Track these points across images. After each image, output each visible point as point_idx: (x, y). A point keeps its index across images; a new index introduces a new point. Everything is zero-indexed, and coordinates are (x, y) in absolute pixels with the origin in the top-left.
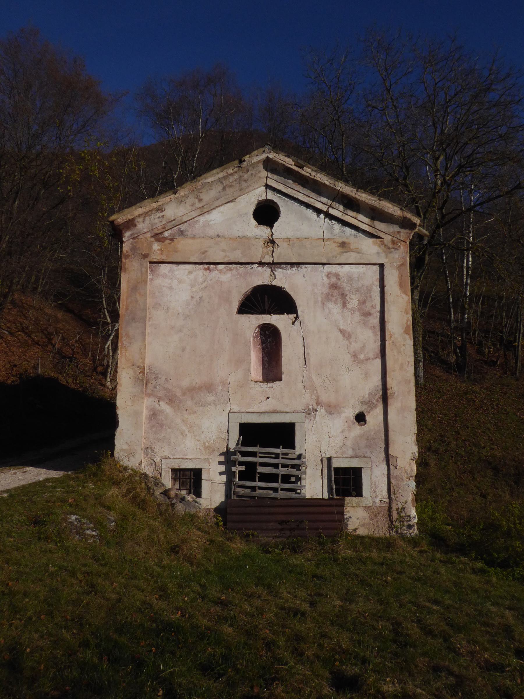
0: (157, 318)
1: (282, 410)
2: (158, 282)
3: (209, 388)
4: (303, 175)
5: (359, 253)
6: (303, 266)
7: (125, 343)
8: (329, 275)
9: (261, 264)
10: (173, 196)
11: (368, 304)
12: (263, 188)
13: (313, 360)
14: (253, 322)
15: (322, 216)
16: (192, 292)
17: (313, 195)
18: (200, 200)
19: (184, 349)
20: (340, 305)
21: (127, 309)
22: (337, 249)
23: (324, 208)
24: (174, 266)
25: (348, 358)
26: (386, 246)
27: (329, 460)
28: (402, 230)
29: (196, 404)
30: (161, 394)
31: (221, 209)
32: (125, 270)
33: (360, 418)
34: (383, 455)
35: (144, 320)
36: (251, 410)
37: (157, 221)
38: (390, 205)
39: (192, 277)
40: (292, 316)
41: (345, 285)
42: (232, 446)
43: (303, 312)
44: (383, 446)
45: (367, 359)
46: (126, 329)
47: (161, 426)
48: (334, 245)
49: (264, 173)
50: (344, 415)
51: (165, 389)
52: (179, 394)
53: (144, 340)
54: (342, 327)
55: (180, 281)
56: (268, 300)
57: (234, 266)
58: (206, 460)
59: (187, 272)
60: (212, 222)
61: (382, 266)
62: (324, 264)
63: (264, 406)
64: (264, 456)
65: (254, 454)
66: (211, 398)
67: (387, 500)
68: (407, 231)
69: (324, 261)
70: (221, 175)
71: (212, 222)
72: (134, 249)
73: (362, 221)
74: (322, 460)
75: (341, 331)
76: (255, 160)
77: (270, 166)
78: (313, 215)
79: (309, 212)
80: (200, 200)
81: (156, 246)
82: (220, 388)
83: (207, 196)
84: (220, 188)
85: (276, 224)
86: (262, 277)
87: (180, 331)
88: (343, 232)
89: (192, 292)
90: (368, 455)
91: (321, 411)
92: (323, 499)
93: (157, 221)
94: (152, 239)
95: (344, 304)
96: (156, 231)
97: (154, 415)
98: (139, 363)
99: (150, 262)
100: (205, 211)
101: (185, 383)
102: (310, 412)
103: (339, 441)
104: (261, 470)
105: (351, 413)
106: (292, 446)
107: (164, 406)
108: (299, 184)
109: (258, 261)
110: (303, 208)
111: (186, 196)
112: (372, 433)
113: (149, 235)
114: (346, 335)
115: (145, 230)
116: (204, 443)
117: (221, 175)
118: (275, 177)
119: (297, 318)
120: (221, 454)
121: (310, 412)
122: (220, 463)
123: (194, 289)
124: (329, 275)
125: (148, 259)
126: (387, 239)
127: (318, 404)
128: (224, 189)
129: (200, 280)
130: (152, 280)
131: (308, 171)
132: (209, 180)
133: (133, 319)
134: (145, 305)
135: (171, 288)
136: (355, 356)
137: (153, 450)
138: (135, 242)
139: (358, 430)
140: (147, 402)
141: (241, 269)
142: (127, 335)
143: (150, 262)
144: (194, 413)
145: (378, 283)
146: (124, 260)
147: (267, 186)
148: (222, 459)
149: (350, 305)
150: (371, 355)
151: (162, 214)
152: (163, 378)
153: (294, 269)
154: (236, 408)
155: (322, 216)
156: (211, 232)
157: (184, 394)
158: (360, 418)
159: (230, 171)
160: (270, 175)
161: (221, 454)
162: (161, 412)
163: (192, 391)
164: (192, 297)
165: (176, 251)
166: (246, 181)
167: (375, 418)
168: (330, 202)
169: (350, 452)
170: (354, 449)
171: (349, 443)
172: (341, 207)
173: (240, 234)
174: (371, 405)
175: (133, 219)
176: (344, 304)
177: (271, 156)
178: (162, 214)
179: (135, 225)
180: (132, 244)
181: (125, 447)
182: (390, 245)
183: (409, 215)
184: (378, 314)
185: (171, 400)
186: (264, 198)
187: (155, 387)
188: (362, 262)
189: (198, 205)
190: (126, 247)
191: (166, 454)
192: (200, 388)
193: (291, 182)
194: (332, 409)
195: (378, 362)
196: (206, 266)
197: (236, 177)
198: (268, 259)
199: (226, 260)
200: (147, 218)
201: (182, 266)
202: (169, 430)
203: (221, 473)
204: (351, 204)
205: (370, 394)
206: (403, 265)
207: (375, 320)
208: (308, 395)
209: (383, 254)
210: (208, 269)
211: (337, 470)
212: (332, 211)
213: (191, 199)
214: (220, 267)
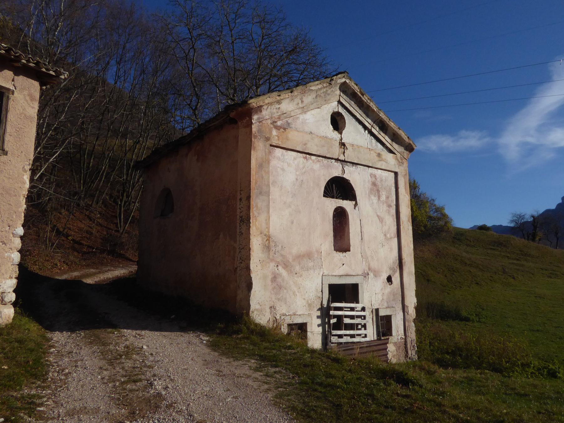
0: (275, 192)
1: (351, 274)
3: (309, 255)
4: (363, 101)
5: (386, 163)
6: (359, 166)
7: (256, 214)
8: (371, 175)
9: (337, 160)
10: (290, 94)
11: (390, 199)
12: (337, 103)
13: (366, 237)
14: (333, 204)
15: (367, 131)
16: (297, 175)
17: (364, 115)
18: (302, 102)
19: (292, 223)
20: (377, 198)
21: (256, 183)
22: (376, 157)
23: (369, 127)
24: (284, 151)
25: (382, 237)
26: (398, 160)
27: (377, 310)
28: (405, 151)
29: (302, 268)
30: (279, 259)
31: (313, 112)
32: (254, 150)
33: (389, 279)
34: (401, 306)
35: (268, 194)
36: (334, 274)
37: (275, 111)
39: (296, 162)
40: (354, 202)
42: (325, 303)
43: (359, 200)
44: (401, 299)
45: (391, 238)
46: (256, 202)
47: (280, 287)
48: (375, 155)
49: (338, 92)
50: (382, 278)
51: (282, 255)
52: (291, 260)
53: (268, 212)
55: (289, 165)
56: (339, 188)
57: (321, 158)
58: (309, 315)
59: (293, 159)
60: (307, 121)
61: (396, 174)
62: (369, 167)
63: (342, 271)
64: (344, 309)
65: (340, 309)
66: (311, 264)
67: (403, 337)
68: (407, 152)
69: (370, 165)
70: (320, 86)
71: (307, 121)
72: (259, 131)
74: (372, 311)
75: (378, 216)
77: (344, 88)
78: (362, 130)
79: (360, 127)
80: (302, 102)
81: (274, 132)
82: (316, 256)
85: (344, 132)
86: (336, 171)
87: (290, 206)
88: (377, 146)
89: (297, 175)
90: (394, 306)
91: (371, 275)
92: (374, 340)
93: (275, 111)
94: (272, 126)
95: (379, 197)
96: (273, 119)
97: (275, 278)
98: (265, 232)
99: (271, 145)
100: (304, 110)
101: (295, 251)
102: (365, 275)
103: (380, 297)
104: (347, 321)
105: (385, 276)
106: (356, 299)
107: (281, 270)
108: (358, 106)
109: (336, 157)
110: (357, 123)
111: (296, 96)
112: (395, 290)
113: (269, 122)
115: (267, 117)
116: (308, 301)
118: (345, 97)
119: (356, 204)
120: (318, 310)
121: (365, 275)
122: (318, 317)
123: (298, 173)
124: (371, 175)
125: (269, 142)
127: (369, 269)
128: (316, 97)
129: (301, 166)
132: (313, 88)
133: (261, 193)
134: (269, 182)
135: (283, 170)
137: (275, 309)
138: (261, 126)
139: (389, 288)
141: (325, 161)
142: (257, 206)
144: (301, 276)
145: (394, 185)
146: (253, 139)
147: (339, 102)
148: (319, 313)
150: (392, 235)
151: (278, 106)
152: (280, 247)
153: (354, 167)
154: (326, 273)
156: (307, 129)
157: (294, 260)
158: (389, 279)
160: (341, 93)
161: (318, 310)
162: (280, 275)
163: (299, 257)
164: (297, 179)
165: (287, 139)
167: (396, 279)
168: (372, 123)
169: (386, 305)
170: (387, 302)
171: (385, 298)
172: (378, 129)
173: (324, 134)
174: (394, 272)
175: (261, 106)
176: (379, 197)
177: (348, 81)
178: (278, 106)
179: (261, 111)
180: (258, 126)
181: (258, 307)
184: (395, 207)
185: (286, 266)
186: (336, 110)
187: (275, 254)
188: (388, 169)
189: (301, 105)
190: (254, 128)
191: (284, 311)
192: (304, 256)
193: (353, 103)
194: (377, 274)
195: (396, 240)
196: (305, 155)
198: (342, 158)
199: (318, 153)
200: (269, 107)
201: (289, 152)
202: (285, 291)
203: (319, 326)
205: (393, 263)
206: (406, 174)
207: (393, 211)
208: (364, 263)
209: (397, 166)
210: (306, 158)
211: (383, 317)
212: (373, 130)
214: (313, 158)
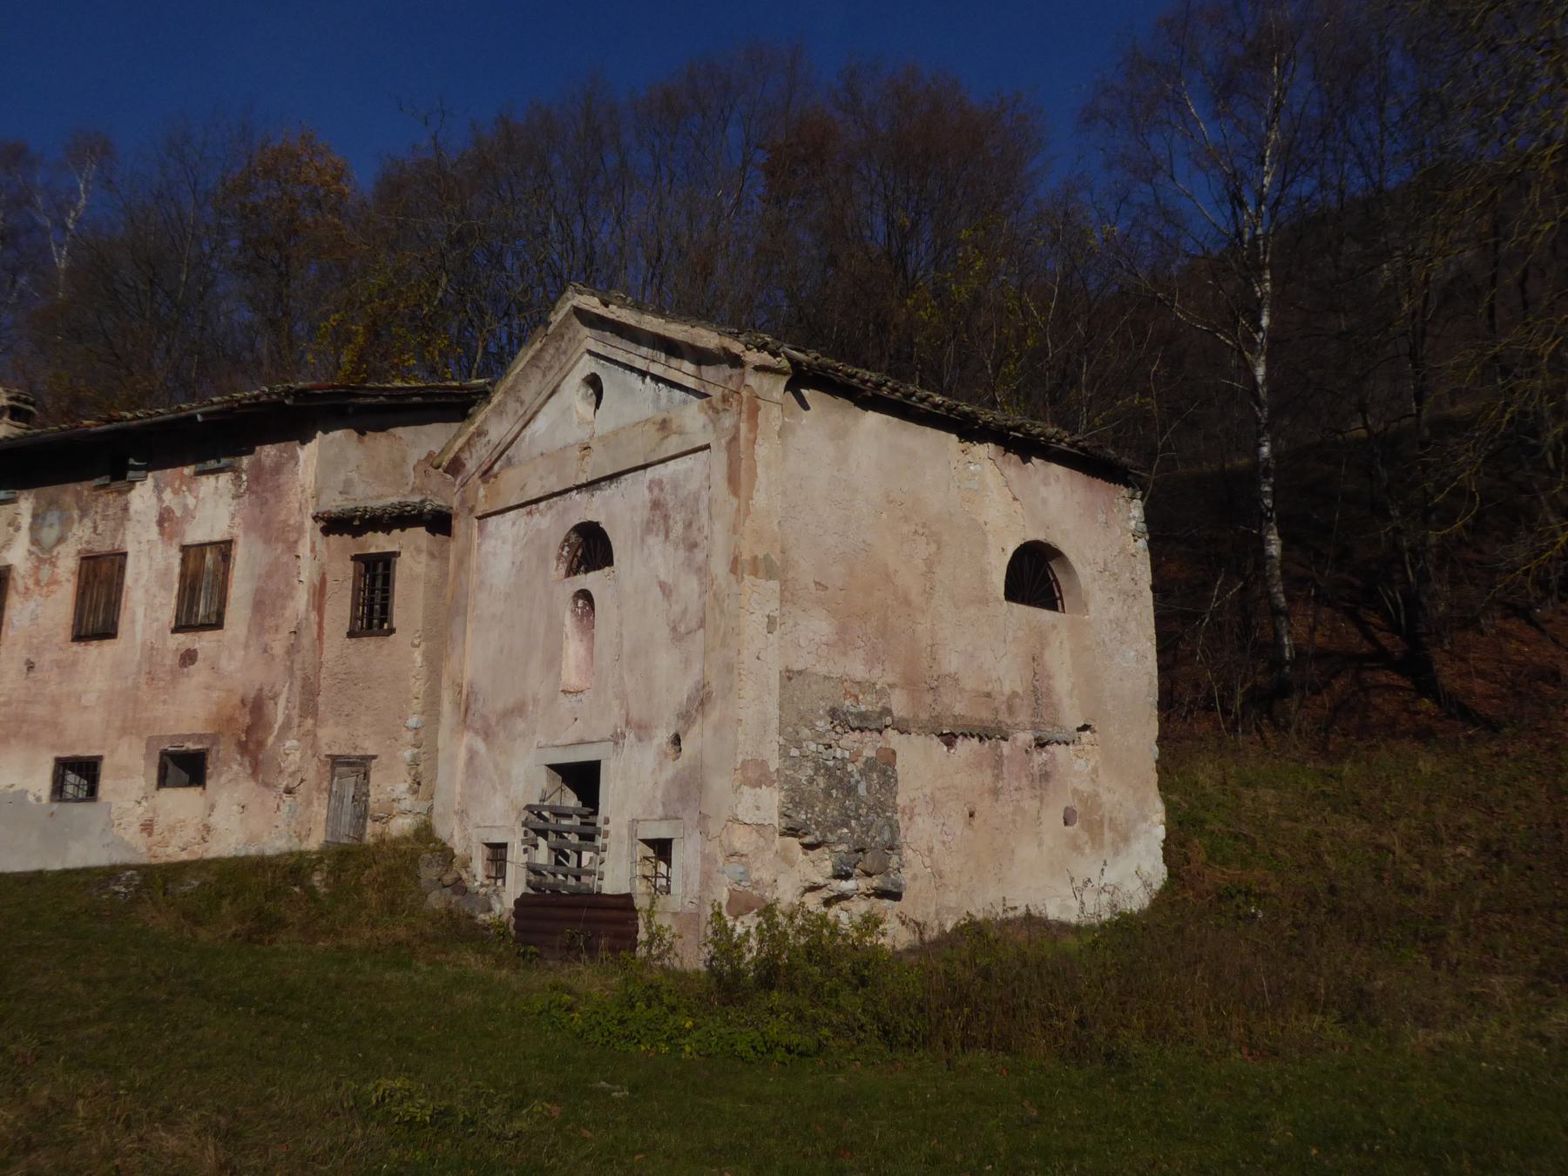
2: (489, 545)
15: (648, 379)
18: (522, 403)
20: (662, 537)
36: (557, 742)
38: (703, 332)
41: (668, 498)
50: (656, 742)
54: (662, 578)
62: (645, 467)
63: (570, 737)
73: (683, 371)
76: (560, 316)
80: (522, 403)
83: (529, 392)
84: (539, 376)
91: (631, 736)
101: (500, 706)
102: (617, 738)
105: (662, 736)
114: (666, 590)
117: (531, 353)
121: (617, 738)
126: (716, 393)
127: (627, 723)
130: (479, 545)
131: (615, 313)
136: (674, 629)
140: (468, 738)
143: (479, 518)
149: (672, 536)
155: (648, 379)
159: (538, 345)
166: (565, 353)
169: (660, 811)
182: (720, 407)
183: (728, 342)
194: (643, 730)
197: (551, 351)
204: (672, 348)
205: (689, 698)
210: (530, 513)
213: (512, 405)
214: (542, 505)
